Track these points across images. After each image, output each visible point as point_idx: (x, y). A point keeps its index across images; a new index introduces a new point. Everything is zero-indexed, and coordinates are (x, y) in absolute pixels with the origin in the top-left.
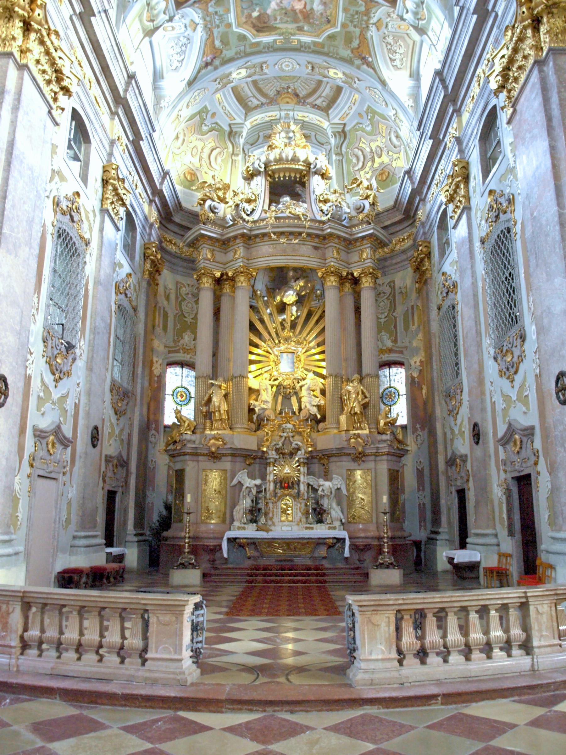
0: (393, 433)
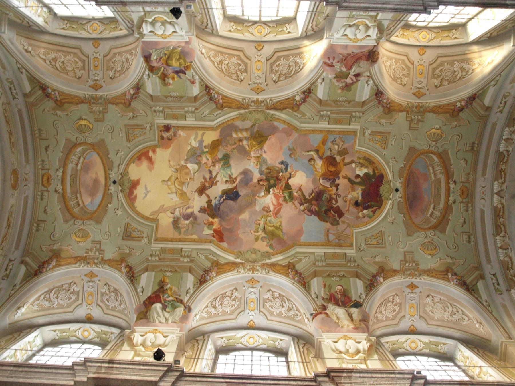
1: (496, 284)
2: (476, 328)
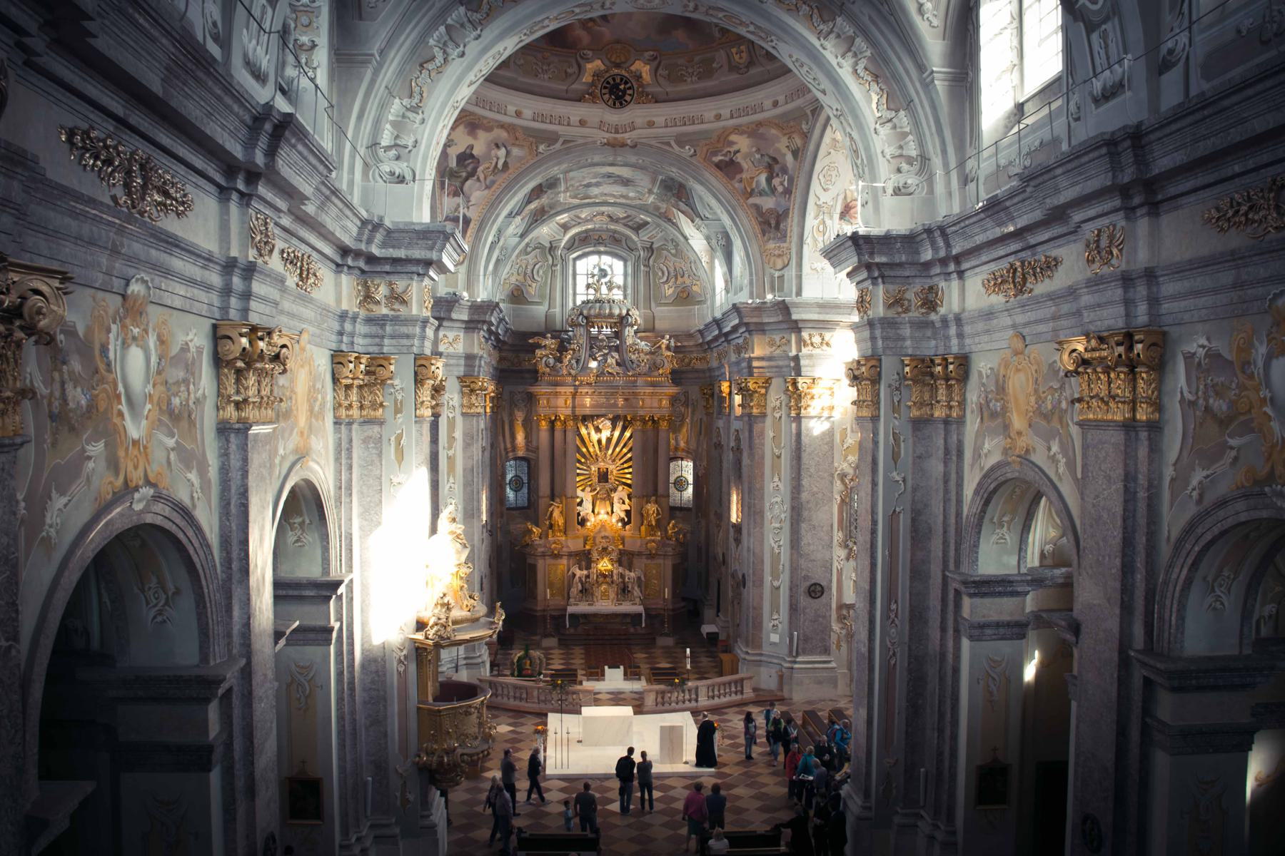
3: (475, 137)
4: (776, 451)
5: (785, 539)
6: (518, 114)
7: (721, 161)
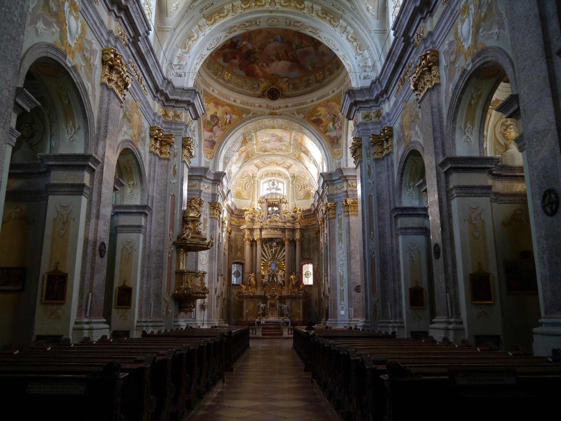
0: (304, 291)
1: (206, 7)
2: (172, 6)
3: (218, 109)
4: (340, 232)
5: (345, 268)
6: (235, 101)
7: (315, 119)
